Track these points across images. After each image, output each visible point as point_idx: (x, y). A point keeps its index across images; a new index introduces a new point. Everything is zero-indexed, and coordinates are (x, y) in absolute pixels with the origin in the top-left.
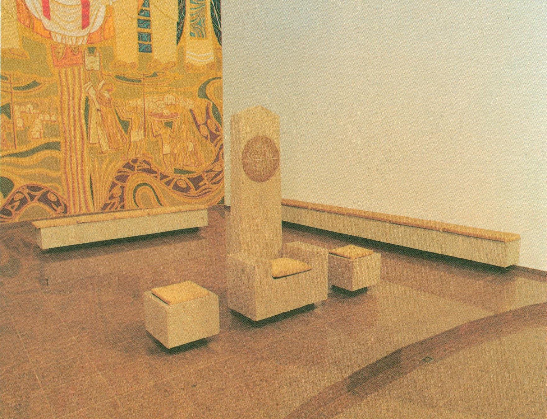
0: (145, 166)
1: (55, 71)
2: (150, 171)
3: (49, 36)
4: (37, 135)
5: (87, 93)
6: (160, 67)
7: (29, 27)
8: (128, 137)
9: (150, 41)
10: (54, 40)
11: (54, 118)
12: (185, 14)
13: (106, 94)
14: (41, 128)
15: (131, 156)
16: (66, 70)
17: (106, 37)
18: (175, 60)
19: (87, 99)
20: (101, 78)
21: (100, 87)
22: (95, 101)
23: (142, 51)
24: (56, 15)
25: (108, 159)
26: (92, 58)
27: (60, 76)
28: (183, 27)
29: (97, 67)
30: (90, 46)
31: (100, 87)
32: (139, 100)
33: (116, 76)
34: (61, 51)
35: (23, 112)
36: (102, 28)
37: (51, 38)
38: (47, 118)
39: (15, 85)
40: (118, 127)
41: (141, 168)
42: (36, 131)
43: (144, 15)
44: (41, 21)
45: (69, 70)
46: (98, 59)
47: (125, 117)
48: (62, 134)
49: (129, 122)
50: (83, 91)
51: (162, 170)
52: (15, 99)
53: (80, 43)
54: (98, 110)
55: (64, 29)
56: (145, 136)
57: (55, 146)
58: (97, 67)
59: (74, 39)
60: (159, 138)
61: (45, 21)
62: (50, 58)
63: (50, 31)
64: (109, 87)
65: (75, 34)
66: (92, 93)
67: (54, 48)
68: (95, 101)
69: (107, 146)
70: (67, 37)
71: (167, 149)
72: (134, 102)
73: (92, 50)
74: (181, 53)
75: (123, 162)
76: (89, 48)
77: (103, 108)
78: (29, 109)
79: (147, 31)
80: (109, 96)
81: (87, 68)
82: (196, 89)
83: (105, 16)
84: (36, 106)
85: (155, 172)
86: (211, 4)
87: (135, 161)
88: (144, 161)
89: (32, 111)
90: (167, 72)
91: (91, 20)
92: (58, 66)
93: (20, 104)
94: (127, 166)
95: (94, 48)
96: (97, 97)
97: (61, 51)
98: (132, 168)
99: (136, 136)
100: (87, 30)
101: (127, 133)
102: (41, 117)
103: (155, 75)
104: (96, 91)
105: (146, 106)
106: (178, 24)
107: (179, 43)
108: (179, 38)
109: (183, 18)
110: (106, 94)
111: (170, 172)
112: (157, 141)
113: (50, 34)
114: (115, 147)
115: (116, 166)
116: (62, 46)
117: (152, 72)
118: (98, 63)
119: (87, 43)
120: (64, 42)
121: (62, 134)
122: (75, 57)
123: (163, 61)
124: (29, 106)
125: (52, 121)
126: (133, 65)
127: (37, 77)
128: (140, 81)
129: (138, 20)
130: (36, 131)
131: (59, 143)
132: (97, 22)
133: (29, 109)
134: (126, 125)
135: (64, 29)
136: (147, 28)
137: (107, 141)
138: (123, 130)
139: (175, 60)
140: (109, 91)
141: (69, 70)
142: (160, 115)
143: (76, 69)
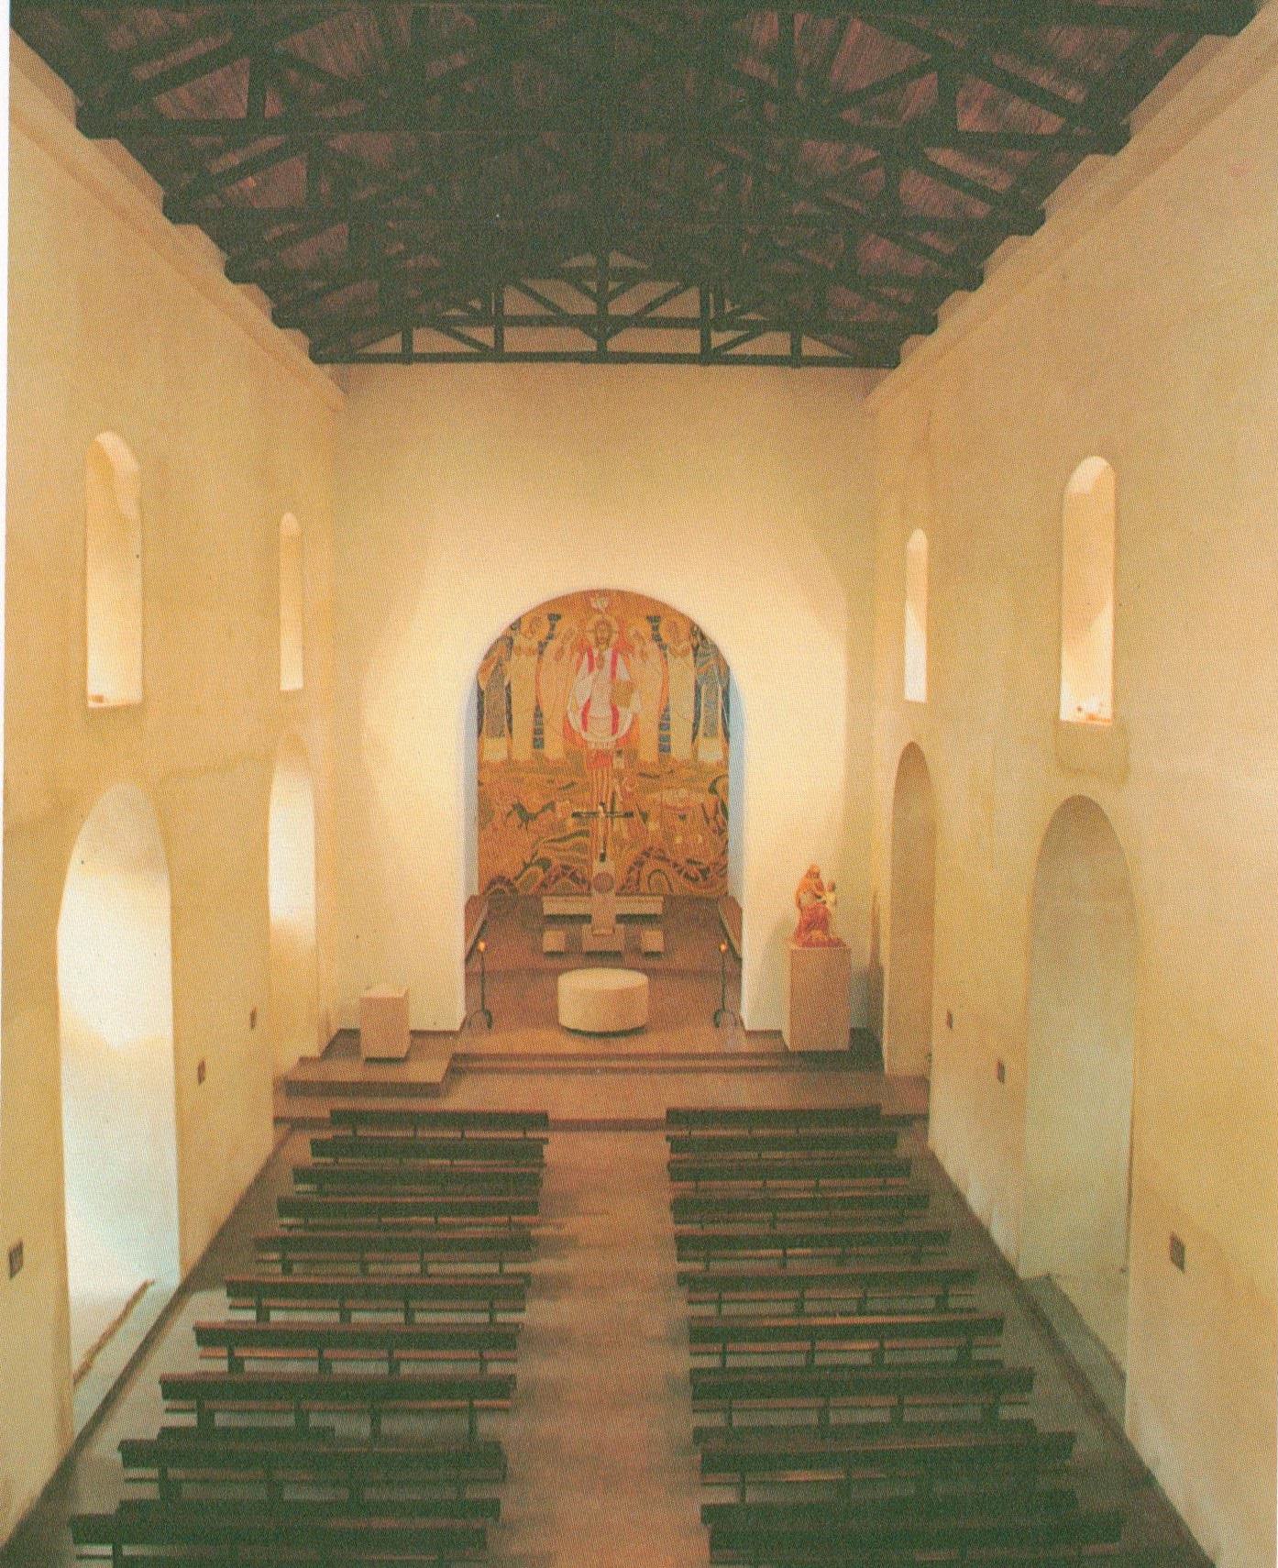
2: (663, 859)
21: (623, 783)
26: (619, 760)
36: (627, 736)
61: (583, 734)
66: (617, 789)
71: (678, 840)
73: (619, 753)
74: (695, 752)
82: (707, 786)
85: (668, 861)
87: (651, 849)
99: (653, 826)
106: (694, 725)
108: (693, 740)
110: (628, 789)
111: (682, 861)
126: (653, 764)
140: (631, 786)
142: (674, 808)
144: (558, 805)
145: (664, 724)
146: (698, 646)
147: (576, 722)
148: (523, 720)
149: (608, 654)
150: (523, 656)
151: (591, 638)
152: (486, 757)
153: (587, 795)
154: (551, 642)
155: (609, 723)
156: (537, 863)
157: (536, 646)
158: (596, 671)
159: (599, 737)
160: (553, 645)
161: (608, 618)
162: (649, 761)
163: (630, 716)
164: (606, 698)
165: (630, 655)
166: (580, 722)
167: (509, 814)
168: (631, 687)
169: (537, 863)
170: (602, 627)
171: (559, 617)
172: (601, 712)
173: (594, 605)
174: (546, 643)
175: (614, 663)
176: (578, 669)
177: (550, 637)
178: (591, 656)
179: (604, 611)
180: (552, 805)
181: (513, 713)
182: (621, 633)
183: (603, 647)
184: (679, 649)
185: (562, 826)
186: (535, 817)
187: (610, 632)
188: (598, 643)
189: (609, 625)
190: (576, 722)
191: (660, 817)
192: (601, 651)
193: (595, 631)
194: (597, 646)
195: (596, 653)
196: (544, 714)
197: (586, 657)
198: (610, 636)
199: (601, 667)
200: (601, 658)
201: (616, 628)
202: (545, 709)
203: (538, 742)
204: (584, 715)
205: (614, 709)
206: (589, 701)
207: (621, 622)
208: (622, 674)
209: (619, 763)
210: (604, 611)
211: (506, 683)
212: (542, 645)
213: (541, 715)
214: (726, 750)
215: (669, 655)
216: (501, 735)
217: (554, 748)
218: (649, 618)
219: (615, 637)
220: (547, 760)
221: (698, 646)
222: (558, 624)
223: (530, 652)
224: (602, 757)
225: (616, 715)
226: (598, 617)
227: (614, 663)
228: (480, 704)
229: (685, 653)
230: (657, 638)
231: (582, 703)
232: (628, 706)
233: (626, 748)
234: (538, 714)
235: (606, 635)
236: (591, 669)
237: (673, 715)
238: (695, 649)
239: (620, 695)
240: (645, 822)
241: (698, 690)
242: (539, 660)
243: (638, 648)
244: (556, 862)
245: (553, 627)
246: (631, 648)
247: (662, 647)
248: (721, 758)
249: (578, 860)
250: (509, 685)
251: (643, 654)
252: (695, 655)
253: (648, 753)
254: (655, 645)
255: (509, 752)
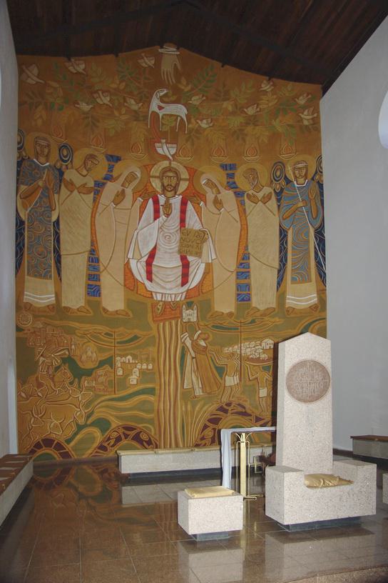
0: (240, 409)
1: (154, 326)
3: (150, 296)
4: (135, 382)
5: (184, 343)
6: (258, 314)
7: (133, 290)
8: (222, 382)
9: (249, 290)
10: (155, 299)
11: (150, 367)
12: (286, 261)
13: (203, 343)
14: (138, 375)
15: (225, 400)
16: (164, 324)
17: (204, 291)
18: (274, 305)
19: (183, 348)
20: (198, 329)
21: (195, 337)
22: (191, 349)
23: (240, 301)
24: (158, 277)
25: (202, 403)
27: (158, 329)
28: (284, 272)
29: (194, 319)
30: (188, 300)
31: (195, 337)
32: (236, 347)
33: (213, 326)
34: (160, 308)
35: (124, 362)
37: (152, 297)
38: (144, 367)
39: (119, 340)
40: (212, 372)
41: (235, 411)
42: (134, 379)
43: (243, 267)
44: (144, 284)
45: (167, 323)
46: (196, 312)
47: (220, 363)
48: (158, 381)
49: (224, 368)
50: (179, 341)
51: (257, 413)
52: (117, 352)
53: (178, 299)
54: (193, 358)
55: (164, 288)
56: (240, 380)
57: (151, 391)
58: (194, 319)
59: (173, 296)
60: (255, 382)
61: (147, 283)
62: (150, 315)
63: (151, 292)
64: (203, 336)
65: (174, 291)
66: (188, 343)
67: (154, 305)
68: (191, 349)
69: (201, 390)
70: (167, 295)
72: (231, 348)
73: (190, 305)
75: (216, 406)
76: (187, 303)
77: (198, 356)
78: (129, 360)
79: (246, 281)
80: (205, 345)
81: (184, 321)
83: (204, 273)
84: (135, 357)
85: (251, 415)
86: (315, 248)
87: (229, 405)
88: (239, 405)
89: (131, 362)
90: (266, 318)
91: (190, 278)
92: (157, 321)
93: (121, 356)
94: (221, 409)
95: (192, 302)
96: (192, 344)
97: (160, 308)
98: (226, 411)
99: (231, 381)
100: (186, 288)
101: (222, 379)
102: (139, 366)
103: (253, 321)
104: (193, 341)
105: (243, 352)
106: (279, 271)
107: (280, 289)
108: (279, 284)
109: (284, 265)
110: (203, 343)
112: (254, 385)
113: (152, 294)
114: (208, 391)
115: (209, 409)
116: (161, 304)
117: (250, 319)
118: (196, 315)
119: (185, 298)
120: (163, 300)
121: (158, 381)
122: (173, 312)
123: (262, 307)
124: (129, 357)
125: (149, 370)
126: (230, 314)
127: (136, 332)
128: (237, 329)
129: (237, 272)
130: (134, 379)
131: (154, 389)
132: (195, 279)
133: (129, 360)
134: (221, 371)
135: (164, 288)
136: (246, 278)
137: (200, 386)
138: (218, 377)
139: (274, 305)
141: (167, 323)
143: (173, 322)
144: (119, 361)
145: (243, 271)
146: (282, 190)
147: (138, 270)
148: (75, 265)
149: (176, 202)
150: (76, 192)
151: (156, 184)
152: (29, 297)
153: (153, 350)
154: (109, 185)
155: (179, 271)
156: (93, 424)
157: (91, 184)
158: (163, 218)
159: (167, 287)
160: (111, 189)
161: (174, 164)
162: (226, 310)
163: (203, 266)
164: (175, 246)
165: (202, 203)
166: (144, 275)
167: (57, 368)
168: (201, 236)
169: (93, 424)
170: (171, 174)
171: (118, 159)
172: (168, 262)
173: (160, 150)
174: (104, 184)
175: (183, 212)
176: (141, 213)
177: (109, 178)
178: (156, 202)
179: (171, 158)
180: (110, 362)
181: (63, 252)
182: (191, 180)
183: (169, 194)
184: (260, 195)
185: (123, 382)
186: (89, 373)
187: (179, 179)
188: (164, 188)
189: (176, 173)
190: (138, 270)
191: (240, 372)
192: (168, 199)
193: (161, 178)
194: (164, 193)
195: (162, 200)
196: (101, 259)
197: (151, 201)
198: (178, 185)
199: (168, 215)
200: (168, 206)
201: (185, 174)
202: (103, 255)
203: (94, 289)
204: (149, 264)
205: (183, 259)
206: (155, 248)
207: (193, 173)
208: (193, 221)
209: (190, 315)
210: (171, 158)
211: (54, 218)
212: (99, 187)
213: (98, 260)
214: (322, 292)
215: (246, 200)
216: (46, 276)
217: (113, 299)
218: (224, 167)
219: (183, 186)
220: (104, 309)
221: (282, 190)
222: (118, 166)
223: (84, 190)
224: (171, 310)
225: (186, 265)
226: (165, 164)
227: (183, 212)
228: (19, 234)
229: (266, 199)
230: (232, 186)
231: (146, 252)
232: (199, 254)
233: (199, 298)
234: (93, 259)
235: (174, 182)
236: (157, 216)
237: (253, 263)
238: (279, 195)
239: (190, 244)
240: (221, 377)
241: (283, 234)
242: (95, 201)
243: (210, 196)
244: (115, 423)
245: (111, 169)
246: (202, 197)
247: (239, 194)
248: (315, 300)
249: (143, 420)
250: (57, 222)
251: (218, 203)
252: (279, 200)
253: (225, 303)
254: (230, 193)
255: (58, 296)
